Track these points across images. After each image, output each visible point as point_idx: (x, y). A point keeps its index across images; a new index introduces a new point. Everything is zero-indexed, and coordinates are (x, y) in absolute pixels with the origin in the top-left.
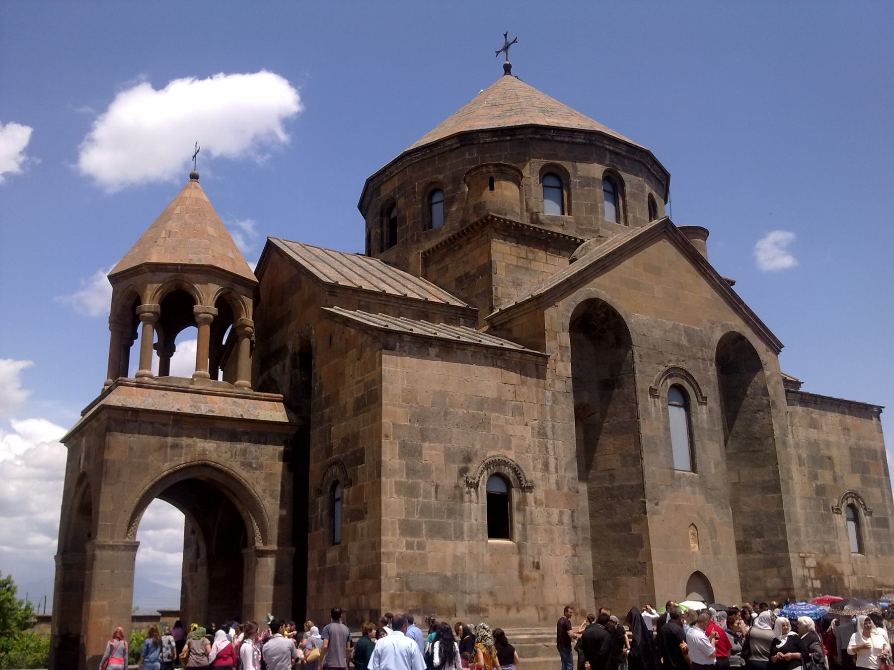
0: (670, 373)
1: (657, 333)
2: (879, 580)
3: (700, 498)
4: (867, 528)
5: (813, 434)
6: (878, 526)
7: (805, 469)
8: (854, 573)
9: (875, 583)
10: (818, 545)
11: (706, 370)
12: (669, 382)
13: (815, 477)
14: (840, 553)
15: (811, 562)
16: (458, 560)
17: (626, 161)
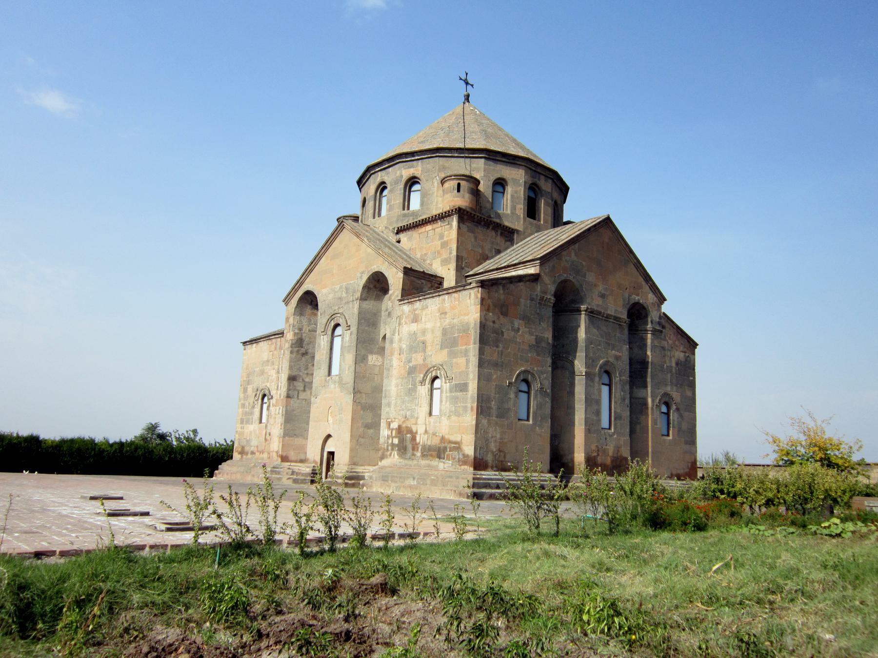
0: (332, 317)
1: (331, 296)
2: (447, 437)
3: (338, 390)
4: (444, 395)
5: (414, 327)
6: (456, 391)
7: (403, 357)
8: (426, 432)
9: (443, 439)
10: (402, 412)
11: (353, 308)
12: (333, 324)
13: (410, 361)
14: (417, 418)
15: (395, 425)
16: (251, 432)
17: (390, 169)
